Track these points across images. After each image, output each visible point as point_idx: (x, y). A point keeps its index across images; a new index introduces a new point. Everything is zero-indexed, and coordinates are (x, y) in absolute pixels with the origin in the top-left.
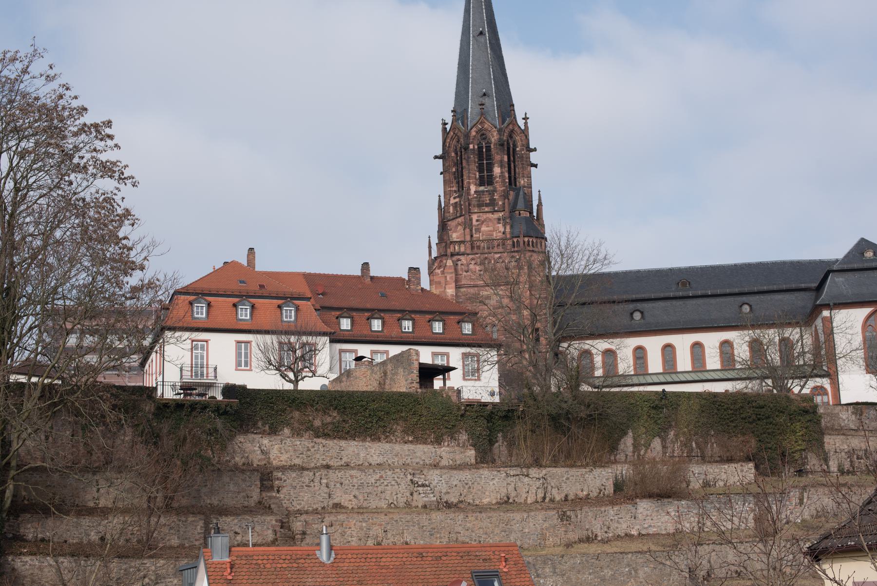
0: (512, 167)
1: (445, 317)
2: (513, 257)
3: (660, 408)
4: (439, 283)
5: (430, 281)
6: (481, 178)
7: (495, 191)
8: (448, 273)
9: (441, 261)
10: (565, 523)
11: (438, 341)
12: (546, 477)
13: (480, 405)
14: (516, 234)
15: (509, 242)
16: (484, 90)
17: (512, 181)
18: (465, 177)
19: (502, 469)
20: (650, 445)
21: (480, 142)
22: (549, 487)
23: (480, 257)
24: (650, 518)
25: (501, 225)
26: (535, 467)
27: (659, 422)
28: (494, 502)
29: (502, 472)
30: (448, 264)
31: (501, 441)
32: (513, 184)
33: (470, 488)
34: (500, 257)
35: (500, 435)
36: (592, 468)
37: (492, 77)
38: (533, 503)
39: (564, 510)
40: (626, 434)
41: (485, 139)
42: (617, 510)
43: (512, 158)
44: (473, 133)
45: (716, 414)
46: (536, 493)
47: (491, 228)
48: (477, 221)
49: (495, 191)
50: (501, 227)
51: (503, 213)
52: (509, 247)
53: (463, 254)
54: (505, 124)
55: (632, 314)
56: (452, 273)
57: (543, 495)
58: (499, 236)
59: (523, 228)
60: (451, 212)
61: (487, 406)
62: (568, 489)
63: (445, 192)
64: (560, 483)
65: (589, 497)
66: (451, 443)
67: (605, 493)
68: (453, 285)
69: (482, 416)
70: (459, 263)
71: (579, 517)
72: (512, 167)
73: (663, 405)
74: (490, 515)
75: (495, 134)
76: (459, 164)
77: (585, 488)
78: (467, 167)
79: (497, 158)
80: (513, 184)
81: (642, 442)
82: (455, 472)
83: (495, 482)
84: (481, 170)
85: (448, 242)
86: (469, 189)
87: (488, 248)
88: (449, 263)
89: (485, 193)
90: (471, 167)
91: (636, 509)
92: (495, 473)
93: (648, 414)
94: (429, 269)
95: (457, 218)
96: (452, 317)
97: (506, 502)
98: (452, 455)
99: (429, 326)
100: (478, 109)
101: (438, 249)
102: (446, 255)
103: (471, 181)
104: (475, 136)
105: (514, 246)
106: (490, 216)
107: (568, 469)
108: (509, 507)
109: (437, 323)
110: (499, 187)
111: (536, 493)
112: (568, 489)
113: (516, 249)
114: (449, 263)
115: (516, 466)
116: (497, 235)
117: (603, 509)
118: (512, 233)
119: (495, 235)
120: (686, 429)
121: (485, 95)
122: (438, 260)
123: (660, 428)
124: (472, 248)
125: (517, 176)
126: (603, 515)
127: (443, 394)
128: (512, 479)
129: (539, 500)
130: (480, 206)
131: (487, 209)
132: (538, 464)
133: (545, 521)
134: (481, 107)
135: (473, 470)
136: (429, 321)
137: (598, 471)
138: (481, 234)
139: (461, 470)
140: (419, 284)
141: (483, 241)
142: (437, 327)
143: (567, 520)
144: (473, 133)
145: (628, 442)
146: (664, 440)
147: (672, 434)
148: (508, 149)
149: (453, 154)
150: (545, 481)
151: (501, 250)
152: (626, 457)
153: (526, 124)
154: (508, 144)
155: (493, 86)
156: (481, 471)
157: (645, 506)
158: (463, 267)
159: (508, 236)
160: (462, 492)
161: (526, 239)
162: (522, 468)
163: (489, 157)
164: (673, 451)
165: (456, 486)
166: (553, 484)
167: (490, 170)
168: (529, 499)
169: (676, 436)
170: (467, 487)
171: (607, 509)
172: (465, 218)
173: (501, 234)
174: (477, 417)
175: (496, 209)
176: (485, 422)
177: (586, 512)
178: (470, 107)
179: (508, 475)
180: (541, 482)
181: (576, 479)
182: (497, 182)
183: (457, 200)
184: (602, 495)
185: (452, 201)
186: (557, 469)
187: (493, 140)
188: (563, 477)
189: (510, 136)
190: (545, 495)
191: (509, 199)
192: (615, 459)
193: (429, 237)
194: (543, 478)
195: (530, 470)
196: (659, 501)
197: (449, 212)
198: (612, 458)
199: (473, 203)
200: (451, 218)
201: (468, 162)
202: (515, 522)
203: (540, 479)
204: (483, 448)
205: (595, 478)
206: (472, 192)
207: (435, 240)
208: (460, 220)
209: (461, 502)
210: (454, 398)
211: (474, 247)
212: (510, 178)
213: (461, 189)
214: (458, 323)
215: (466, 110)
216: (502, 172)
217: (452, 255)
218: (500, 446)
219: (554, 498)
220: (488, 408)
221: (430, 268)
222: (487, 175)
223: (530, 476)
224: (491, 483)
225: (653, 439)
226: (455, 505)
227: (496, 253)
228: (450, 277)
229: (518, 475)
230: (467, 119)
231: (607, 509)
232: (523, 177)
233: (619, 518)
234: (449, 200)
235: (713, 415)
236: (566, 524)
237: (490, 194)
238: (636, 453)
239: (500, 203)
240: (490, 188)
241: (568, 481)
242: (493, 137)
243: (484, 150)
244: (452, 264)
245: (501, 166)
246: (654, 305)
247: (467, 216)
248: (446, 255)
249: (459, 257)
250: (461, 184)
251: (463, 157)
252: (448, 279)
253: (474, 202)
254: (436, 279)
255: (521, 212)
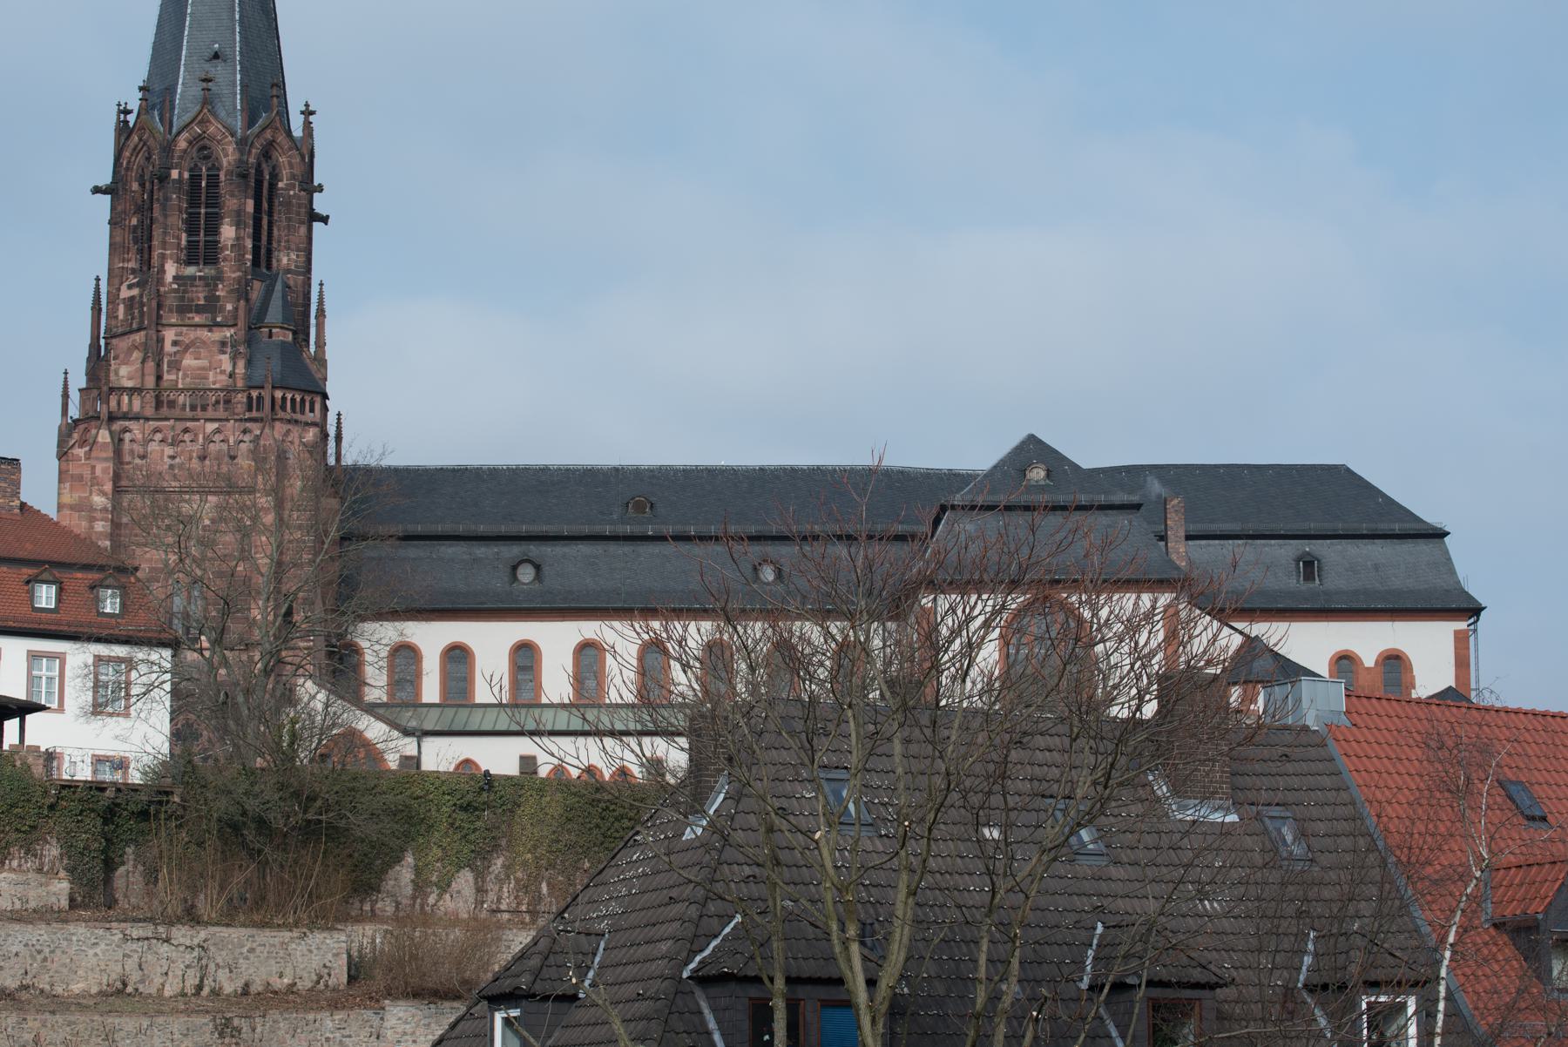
0: (265, 227)
1: (64, 575)
2: (245, 432)
3: (476, 809)
4: (80, 478)
5: (61, 473)
6: (192, 245)
7: (219, 278)
8: (97, 459)
9: (87, 430)
10: (227, 1040)
11: (41, 626)
12: (205, 945)
13: (91, 788)
14: (257, 381)
15: (241, 398)
16: (217, 46)
17: (262, 258)
18: (155, 243)
19: (114, 925)
20: (449, 885)
21: (196, 165)
22: (212, 966)
23: (173, 428)
24: (411, 1039)
25: (227, 356)
26: (183, 924)
27: (472, 837)
28: (94, 990)
29: (115, 931)
30: (100, 439)
31: (131, 863)
32: (263, 264)
33: (45, 959)
34: (218, 431)
35: (129, 850)
36: (305, 930)
37: (237, 17)
38: (175, 996)
39: (228, 1015)
40: (399, 860)
41: (207, 158)
42: (341, 1020)
43: (265, 205)
44: (182, 144)
45: (597, 826)
46: (183, 975)
47: (204, 363)
48: (175, 343)
49: (219, 278)
50: (225, 361)
51: (232, 331)
52: (240, 408)
53: (136, 418)
54: (256, 129)
55: (515, 568)
56: (106, 459)
57: (197, 982)
58: (221, 381)
59: (276, 365)
60: (121, 317)
61: (103, 790)
62: (251, 971)
63: (110, 271)
64: (235, 958)
65: (295, 989)
66: (26, 862)
67: (330, 983)
68: (108, 487)
69: (93, 810)
70: (127, 436)
71: (259, 1030)
72: (265, 227)
73: (484, 803)
74: (72, 1018)
75: (230, 149)
76: (144, 209)
77: (288, 971)
78: (161, 219)
79: (230, 203)
80: (263, 264)
81: (434, 878)
82: (17, 927)
83: (98, 950)
84: (192, 229)
85: (105, 389)
86: (162, 271)
87: (193, 408)
88: (104, 436)
89: (197, 282)
90: (170, 220)
91: (382, 1019)
92: (101, 932)
93: (450, 820)
94: (58, 447)
95: (131, 332)
96: (79, 575)
97: (120, 993)
98: (20, 888)
99: (28, 592)
100: (196, 90)
101: (83, 402)
102: (98, 418)
103: (168, 252)
104: (185, 151)
105: (250, 409)
106: (204, 334)
107: (250, 931)
108: (117, 1002)
109: (45, 586)
110: (230, 272)
111: (183, 975)
112: (251, 971)
113: (254, 414)
114: (104, 436)
115: (145, 921)
116: (216, 380)
117: (311, 1017)
118: (247, 377)
119: (211, 379)
120: (529, 856)
121: (216, 56)
122: (82, 427)
123: (472, 851)
124: (159, 404)
125: (275, 245)
126: (310, 1028)
127: (15, 761)
128: (134, 946)
129: (190, 990)
130: (183, 310)
131: (197, 319)
132: (191, 917)
133: (185, 1035)
134: (204, 85)
135: (54, 925)
136: (28, 582)
137: (317, 937)
138: (181, 374)
139: (31, 923)
140: (16, 494)
141: (182, 390)
142: (44, 595)
143: (233, 1036)
144: (182, 144)
145: (403, 874)
146: (480, 876)
147: (499, 863)
148: (259, 183)
149: (135, 186)
150: (203, 954)
151: (221, 413)
152: (397, 907)
153: (308, 126)
154: (259, 171)
155: (238, 38)
156: (71, 928)
157: (401, 1014)
158: (135, 446)
159: (240, 384)
160: (28, 967)
161: (279, 394)
162: (157, 924)
163: (214, 201)
164: (499, 900)
165: (17, 955)
166: (219, 960)
167: (213, 229)
168: (167, 987)
169: (507, 868)
170: (39, 957)
171: (319, 1017)
172: (146, 335)
173: (224, 378)
174: (82, 811)
175: (219, 319)
176: (99, 821)
177: (274, 1022)
178: (181, 81)
179: (126, 938)
180: (195, 954)
181: (268, 952)
182: (225, 260)
183: (135, 292)
184: (321, 986)
185: (125, 293)
186: (231, 930)
187: (225, 162)
188: (243, 946)
189: (266, 154)
190: (202, 980)
191: (247, 300)
192: (372, 910)
193: (66, 373)
194: (199, 946)
195: (174, 929)
196: (432, 1006)
197: (117, 317)
198: (367, 907)
199: (168, 302)
200: (120, 330)
201: (164, 208)
202: (122, 1034)
203: (193, 949)
204: (89, 875)
205: (311, 951)
206: (169, 277)
207: (79, 380)
208: (138, 337)
209: (25, 987)
210: (38, 770)
211: (162, 402)
212: (256, 250)
213: (145, 268)
214: (92, 588)
215: (171, 90)
216: (238, 238)
217: (112, 418)
218: (128, 872)
219: (220, 988)
220: (108, 793)
221: (62, 443)
222: (206, 241)
223: (173, 941)
224: (91, 952)
225: (457, 872)
226: (9, 995)
227: (207, 420)
228: (104, 469)
229: (147, 939)
230: (173, 108)
231: (319, 1017)
232: (289, 248)
233: (343, 1036)
234: (119, 290)
235: (590, 829)
236: (230, 1044)
237: (207, 285)
238: (419, 901)
239: (229, 307)
240: (209, 271)
241: (251, 956)
242: (226, 155)
243: (204, 184)
244: (109, 440)
245: (238, 224)
246: (566, 550)
247: (152, 332)
248: (98, 418)
249: (127, 423)
250: (146, 256)
251: (155, 197)
252: (98, 471)
253: (171, 301)
254: (73, 469)
255: (274, 330)
